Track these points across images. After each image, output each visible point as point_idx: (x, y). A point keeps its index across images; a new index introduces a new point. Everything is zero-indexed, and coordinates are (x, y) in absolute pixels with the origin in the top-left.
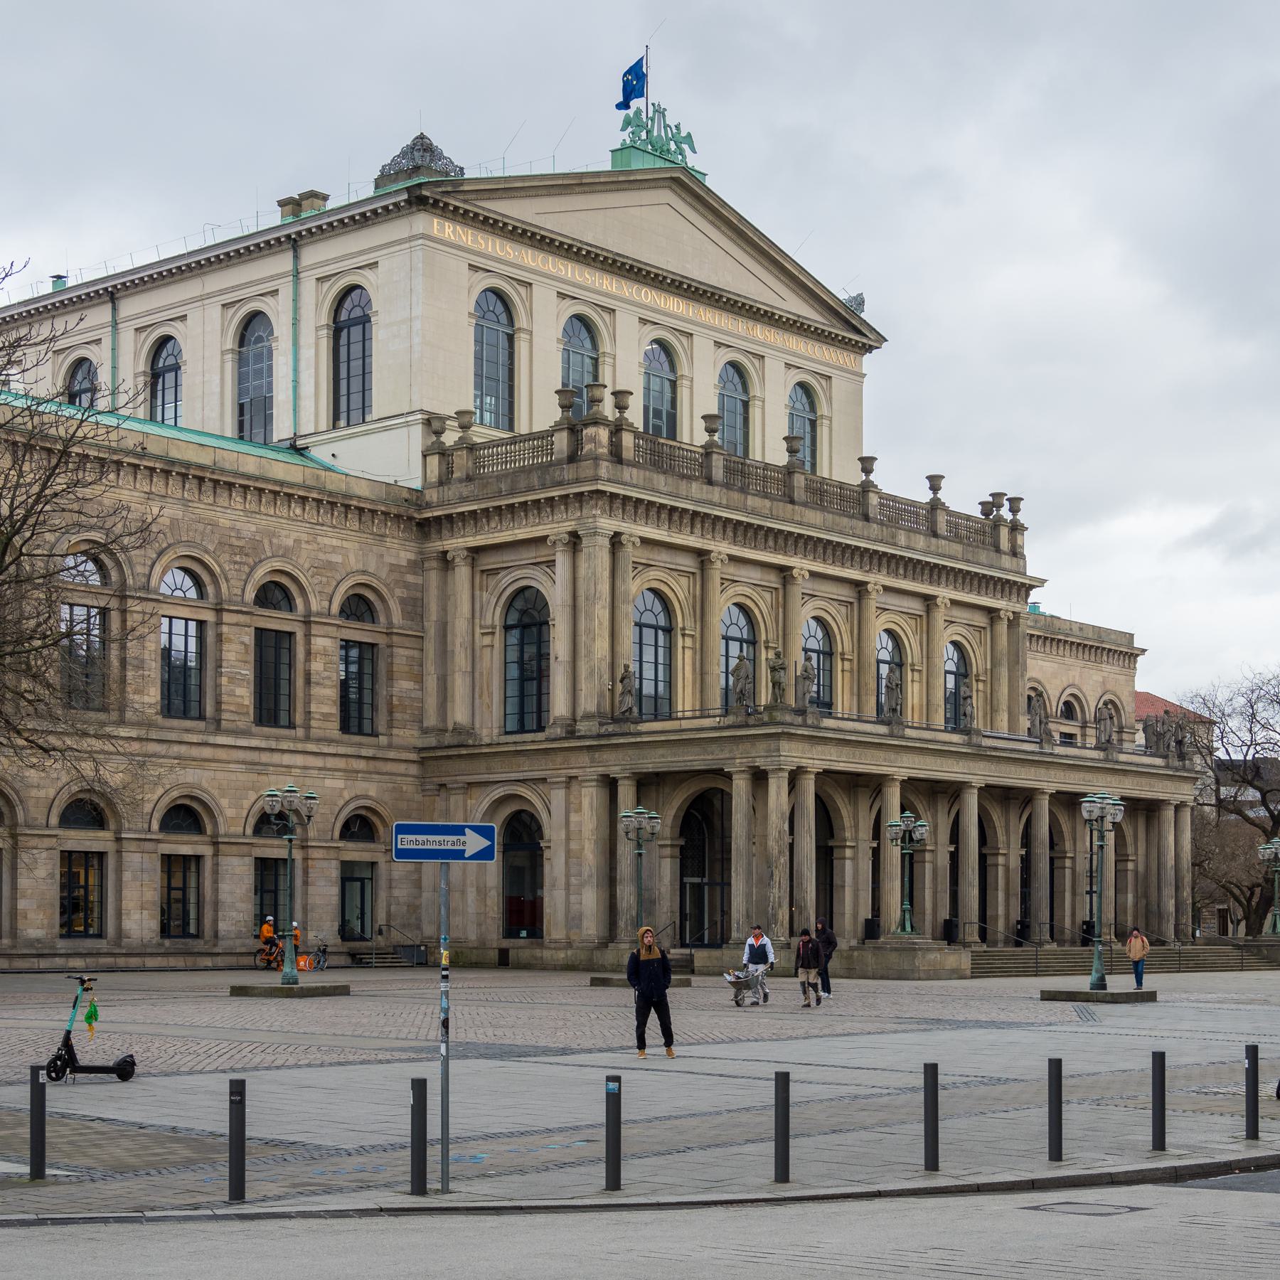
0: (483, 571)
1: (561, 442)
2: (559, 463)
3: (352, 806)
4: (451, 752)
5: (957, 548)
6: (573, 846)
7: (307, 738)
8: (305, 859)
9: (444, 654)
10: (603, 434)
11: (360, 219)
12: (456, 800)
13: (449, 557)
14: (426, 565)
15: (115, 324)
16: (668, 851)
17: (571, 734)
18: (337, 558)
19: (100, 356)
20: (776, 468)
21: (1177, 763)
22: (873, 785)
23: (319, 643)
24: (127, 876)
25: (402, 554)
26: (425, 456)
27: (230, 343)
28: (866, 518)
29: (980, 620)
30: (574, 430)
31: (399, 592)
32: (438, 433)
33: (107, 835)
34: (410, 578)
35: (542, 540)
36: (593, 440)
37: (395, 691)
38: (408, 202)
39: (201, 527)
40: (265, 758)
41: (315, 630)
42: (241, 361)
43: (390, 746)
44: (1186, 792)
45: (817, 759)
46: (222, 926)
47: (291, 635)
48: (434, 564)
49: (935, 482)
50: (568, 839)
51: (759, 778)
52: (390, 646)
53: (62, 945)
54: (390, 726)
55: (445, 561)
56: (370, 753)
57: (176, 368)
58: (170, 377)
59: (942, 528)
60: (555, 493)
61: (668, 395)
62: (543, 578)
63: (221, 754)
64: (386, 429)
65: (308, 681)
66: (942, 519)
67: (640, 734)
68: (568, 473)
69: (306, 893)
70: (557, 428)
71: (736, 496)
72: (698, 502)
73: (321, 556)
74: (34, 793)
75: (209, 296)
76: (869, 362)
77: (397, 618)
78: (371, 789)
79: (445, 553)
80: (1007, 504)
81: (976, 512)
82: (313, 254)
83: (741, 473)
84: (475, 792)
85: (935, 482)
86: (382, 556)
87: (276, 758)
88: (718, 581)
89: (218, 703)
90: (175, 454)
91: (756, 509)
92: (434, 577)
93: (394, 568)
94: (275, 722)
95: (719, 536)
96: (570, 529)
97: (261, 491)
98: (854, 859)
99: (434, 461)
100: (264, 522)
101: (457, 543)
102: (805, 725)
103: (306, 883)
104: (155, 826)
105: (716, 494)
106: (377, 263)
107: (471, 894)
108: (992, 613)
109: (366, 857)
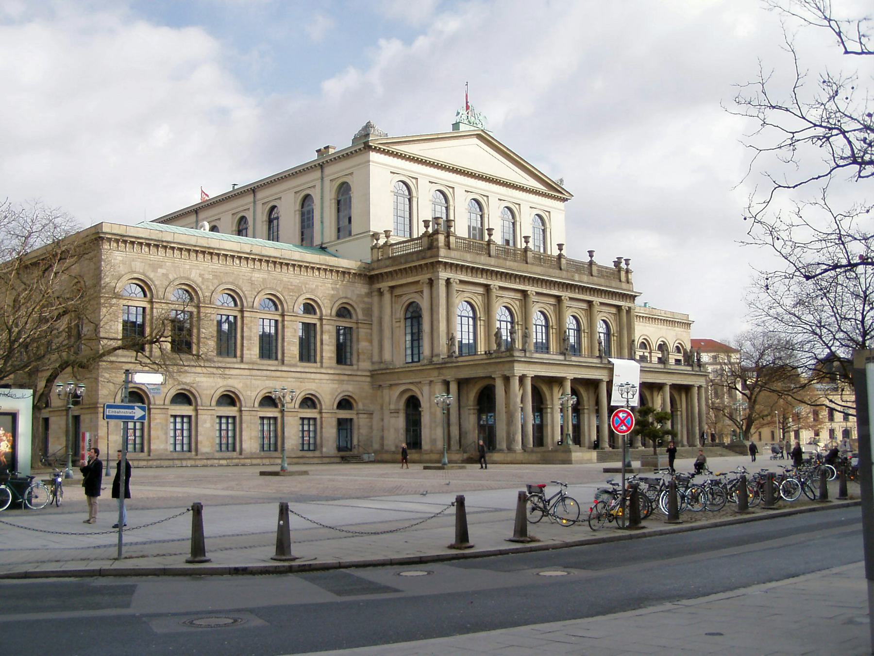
3: (341, 395)
4: (384, 372)
5: (602, 281)
6: (433, 410)
9: (381, 331)
11: (345, 156)
12: (386, 392)
15: (255, 202)
16: (472, 411)
17: (431, 362)
19: (249, 216)
21: (697, 369)
22: (559, 381)
23: (326, 328)
24: (244, 426)
27: (298, 207)
28: (561, 269)
29: (614, 310)
31: (361, 306)
32: (377, 240)
33: (236, 409)
34: (366, 300)
35: (418, 282)
36: (437, 240)
37: (360, 347)
40: (304, 375)
42: (303, 214)
43: (358, 370)
44: (701, 381)
45: (531, 371)
47: (315, 325)
48: (376, 293)
49: (591, 253)
50: (430, 407)
51: (507, 379)
52: (358, 328)
53: (218, 455)
54: (358, 361)
55: (380, 293)
56: (349, 373)
57: (277, 218)
58: (275, 222)
59: (595, 272)
60: (422, 262)
61: (479, 222)
63: (284, 374)
64: (358, 239)
66: (594, 268)
67: (458, 362)
68: (429, 253)
71: (501, 261)
72: (483, 265)
74: (205, 392)
75: (289, 189)
77: (361, 316)
78: (349, 389)
80: (624, 262)
81: (612, 266)
82: (329, 170)
84: (393, 387)
85: (591, 253)
87: (308, 375)
89: (283, 353)
90: (264, 253)
92: (376, 299)
93: (359, 296)
94: (309, 361)
95: (494, 278)
97: (300, 266)
98: (552, 413)
100: (302, 278)
101: (384, 285)
102: (525, 357)
103: (321, 428)
104: (257, 404)
107: (392, 430)
108: (619, 308)
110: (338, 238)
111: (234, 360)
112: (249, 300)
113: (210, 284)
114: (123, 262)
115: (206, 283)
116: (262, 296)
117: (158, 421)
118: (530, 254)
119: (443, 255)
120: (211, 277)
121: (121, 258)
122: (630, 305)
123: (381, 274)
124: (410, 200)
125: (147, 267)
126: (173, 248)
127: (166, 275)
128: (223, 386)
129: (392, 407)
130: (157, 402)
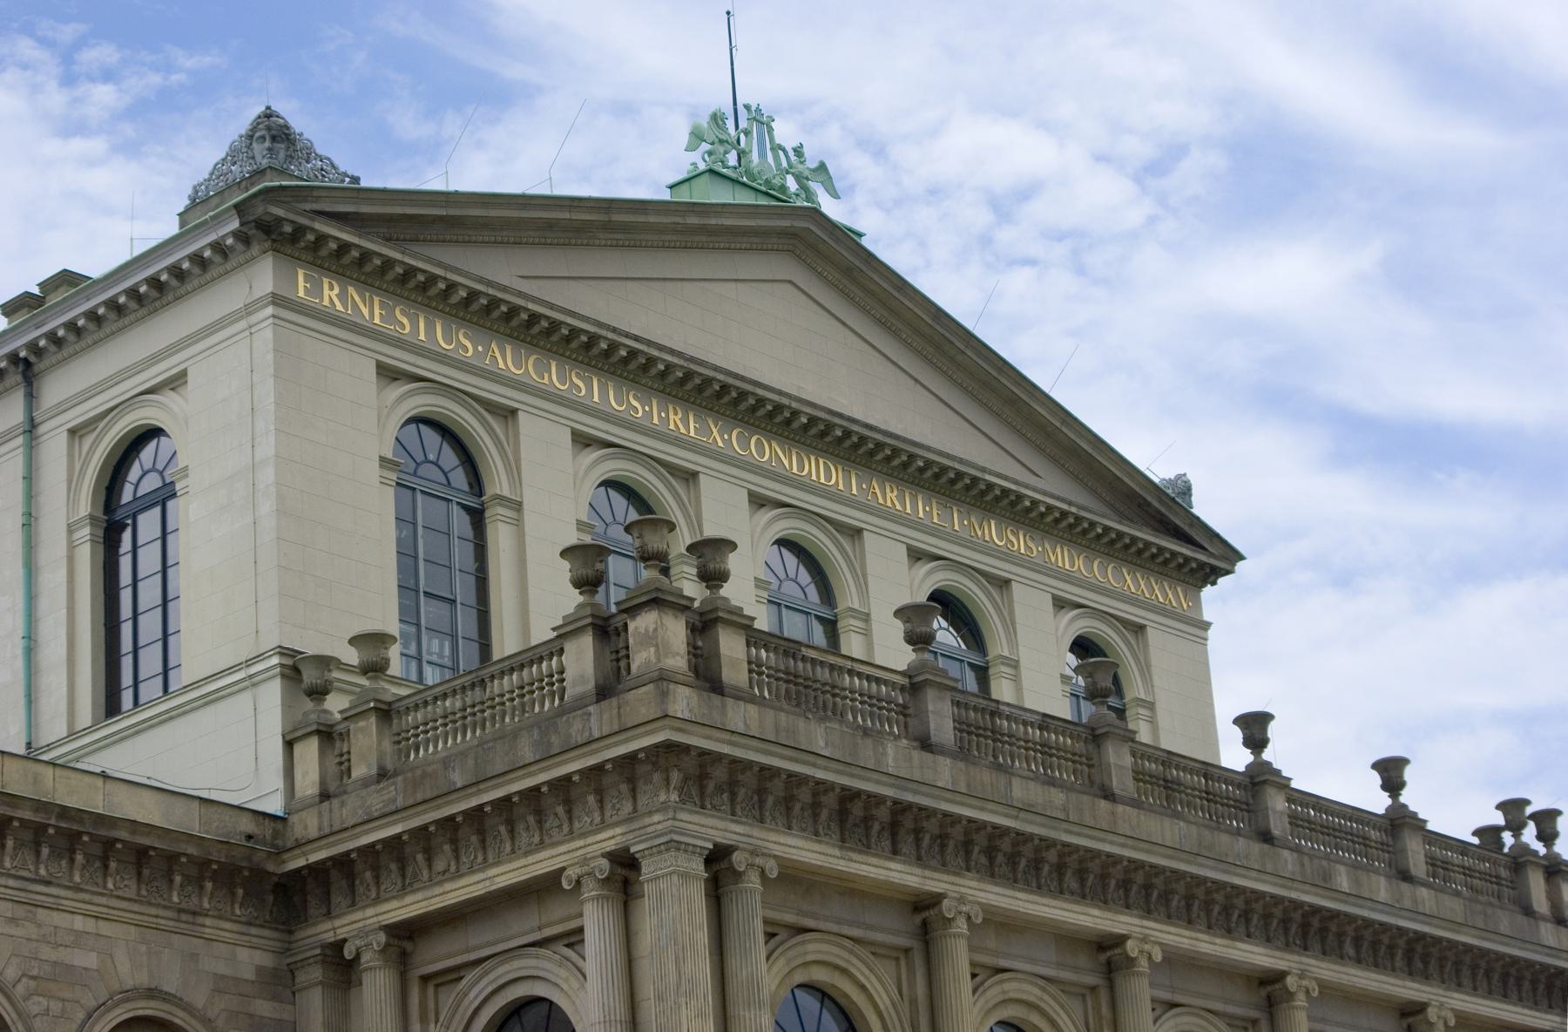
0: (425, 979)
1: (581, 662)
2: (580, 704)
5: (1454, 907)
10: (676, 631)
13: (348, 952)
14: (302, 978)
18: (87, 960)
25: (243, 954)
26: (289, 745)
28: (1266, 837)
30: (606, 631)
32: (318, 693)
38: (242, 237)
48: (316, 973)
49: (1391, 773)
55: (342, 968)
62: (561, 974)
68: (600, 719)
70: (566, 633)
71: (985, 776)
73: (47, 953)
76: (1214, 600)
79: (339, 945)
83: (987, 729)
85: (1391, 773)
86: (194, 956)
88: (965, 970)
91: (1027, 802)
92: (314, 1005)
93: (221, 985)
96: (610, 846)
99: (309, 752)
101: (362, 923)
105: (944, 771)
106: (183, 374)
110: (112, 707)
123: (343, 862)
124: (477, 517)
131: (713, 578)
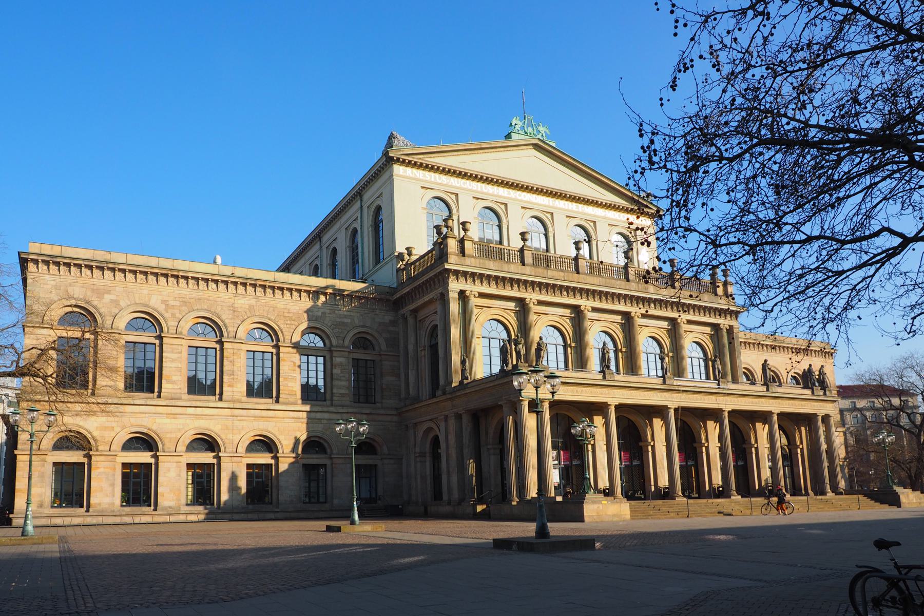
7: (332, 405)
8: (332, 464)
20: (568, 258)
28: (628, 280)
34: (391, 329)
39: (266, 308)
41: (335, 354)
46: (281, 498)
65: (332, 379)
69: (332, 481)
74: (168, 436)
108: (716, 327)
109: (370, 462)
111: (212, 398)
112: (230, 329)
113: (176, 311)
114: (57, 287)
115: (170, 311)
116: (247, 326)
117: (102, 470)
118: (582, 263)
119: (453, 262)
120: (178, 303)
121: (53, 283)
122: (733, 323)
125: (89, 293)
126: (124, 271)
127: (116, 302)
128: (195, 428)
129: (418, 450)
130: (100, 448)
131: (465, 230)
